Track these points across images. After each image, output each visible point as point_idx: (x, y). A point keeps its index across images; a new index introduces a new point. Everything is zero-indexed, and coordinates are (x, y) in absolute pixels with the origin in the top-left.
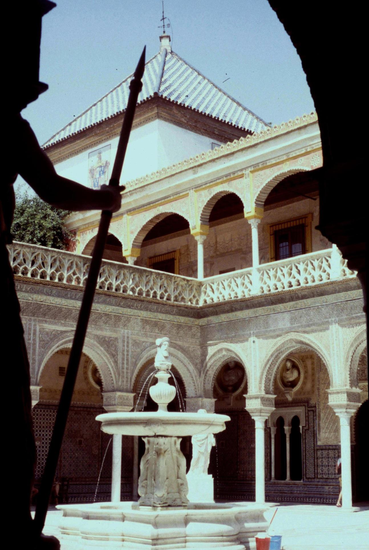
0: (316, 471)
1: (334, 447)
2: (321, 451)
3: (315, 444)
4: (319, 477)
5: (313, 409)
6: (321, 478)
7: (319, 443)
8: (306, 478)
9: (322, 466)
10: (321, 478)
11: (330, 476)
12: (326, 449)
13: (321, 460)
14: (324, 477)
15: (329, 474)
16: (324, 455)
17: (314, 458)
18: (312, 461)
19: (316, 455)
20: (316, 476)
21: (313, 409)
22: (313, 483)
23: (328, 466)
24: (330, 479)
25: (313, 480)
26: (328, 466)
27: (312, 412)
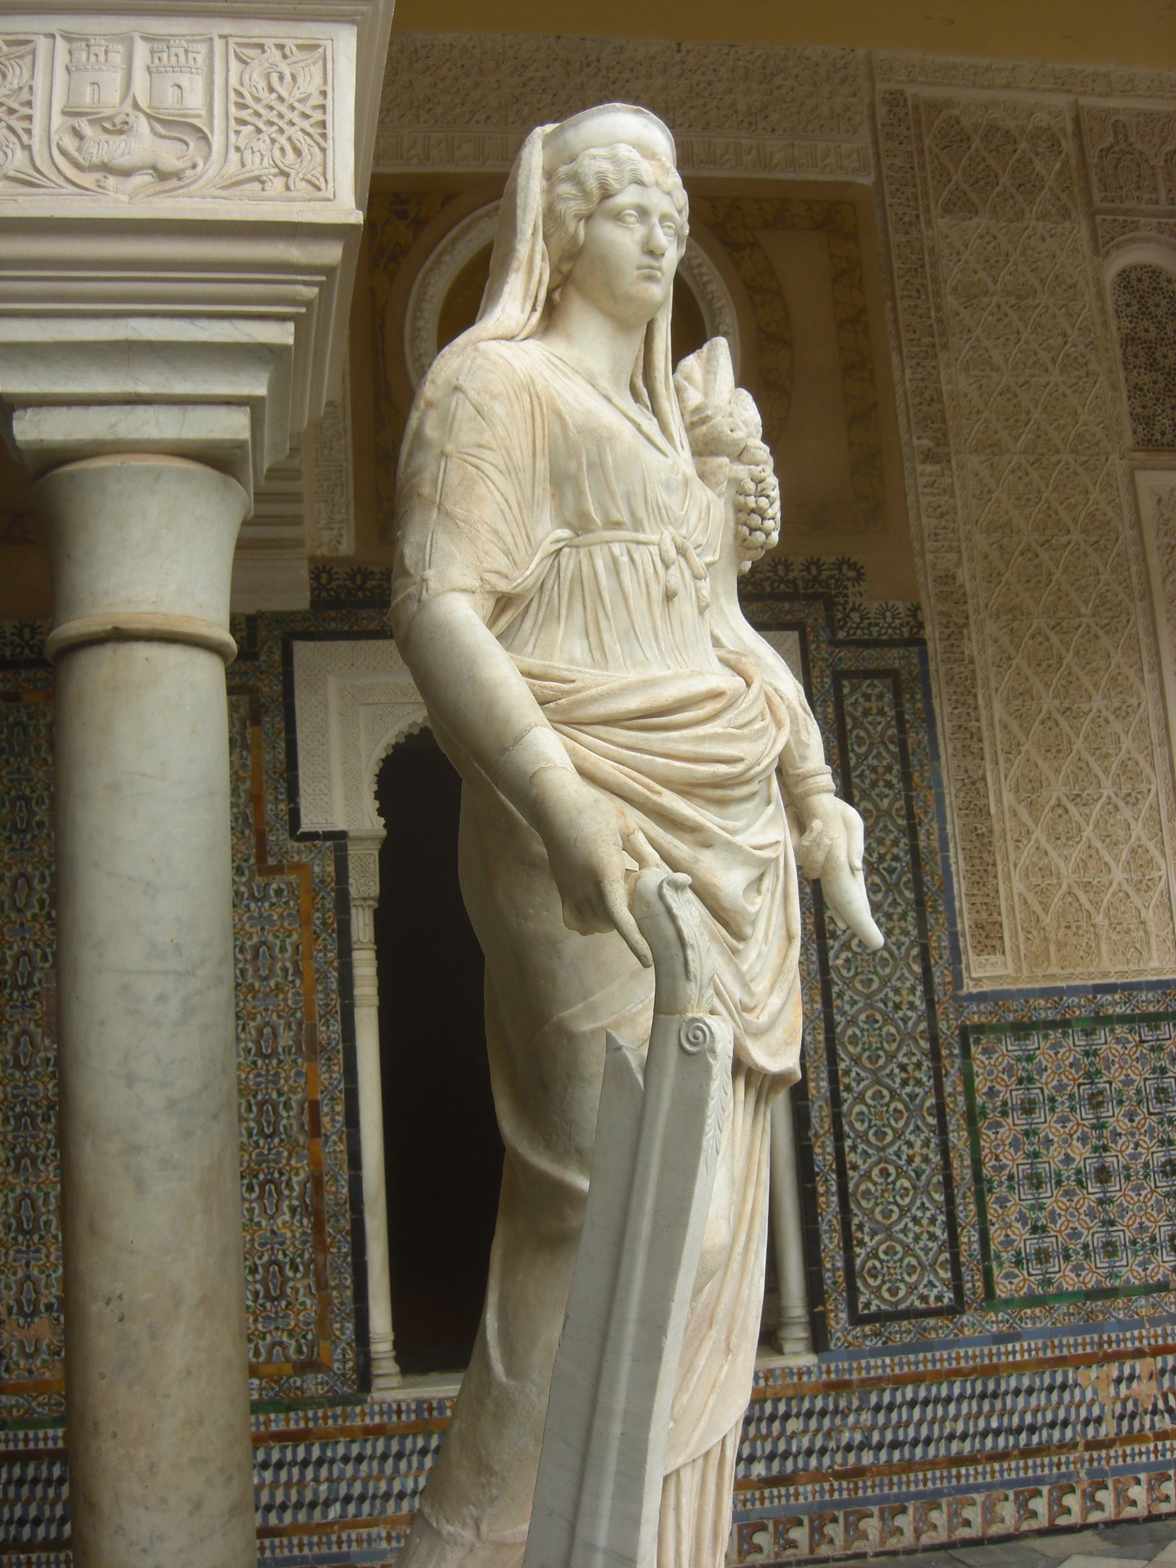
0: (969, 1237)
1: (1148, 1003)
2: (1009, 1047)
3: (940, 976)
4: (1002, 1289)
5: (893, 658)
6: (1032, 1300)
7: (985, 972)
8: (857, 1319)
9: (1036, 1182)
10: (1032, 1300)
11: (1130, 1270)
12: (1064, 1024)
13: (1015, 1123)
14: (1069, 1281)
15: (1110, 1249)
16: (1047, 1083)
17: (940, 1111)
18: (919, 1144)
19: (952, 1084)
20: (973, 1283)
21: (893, 658)
22: (944, 1359)
23: (1103, 1175)
24: (1129, 1292)
25: (938, 1329)
26: (1103, 1175)
27: (879, 686)
